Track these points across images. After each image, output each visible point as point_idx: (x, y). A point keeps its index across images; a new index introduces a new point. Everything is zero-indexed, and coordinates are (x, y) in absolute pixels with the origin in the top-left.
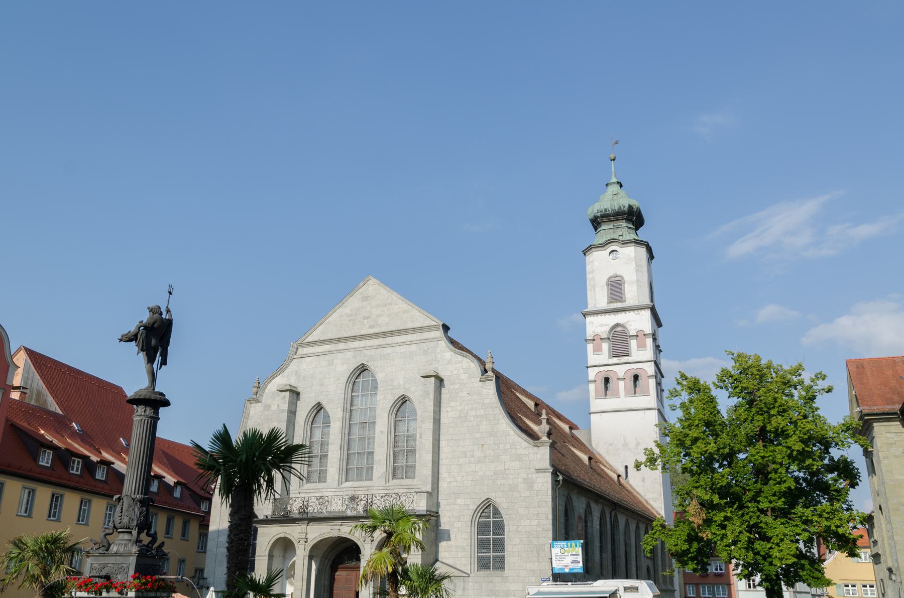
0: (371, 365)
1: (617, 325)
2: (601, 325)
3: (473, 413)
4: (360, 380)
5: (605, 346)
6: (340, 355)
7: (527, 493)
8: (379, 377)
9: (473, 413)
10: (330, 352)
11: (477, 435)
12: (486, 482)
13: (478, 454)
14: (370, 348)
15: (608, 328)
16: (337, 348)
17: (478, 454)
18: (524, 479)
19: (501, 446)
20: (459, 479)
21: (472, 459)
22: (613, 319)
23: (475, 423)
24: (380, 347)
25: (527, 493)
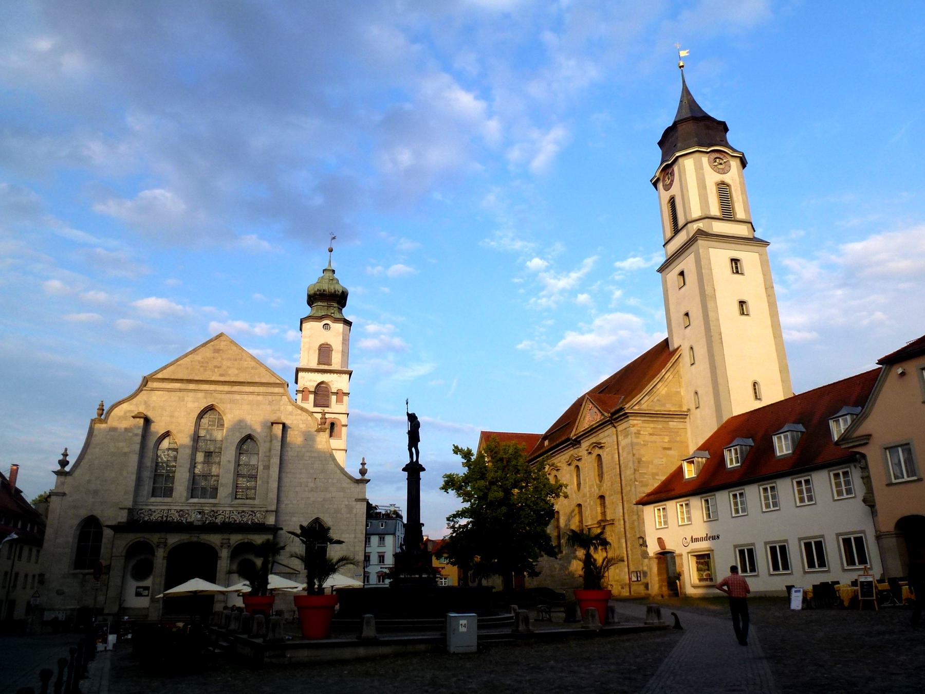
0: (220, 407)
1: (322, 383)
2: (310, 381)
5: (312, 397)
9: (308, 454)
11: (312, 471)
15: (315, 384)
20: (295, 502)
22: (320, 378)
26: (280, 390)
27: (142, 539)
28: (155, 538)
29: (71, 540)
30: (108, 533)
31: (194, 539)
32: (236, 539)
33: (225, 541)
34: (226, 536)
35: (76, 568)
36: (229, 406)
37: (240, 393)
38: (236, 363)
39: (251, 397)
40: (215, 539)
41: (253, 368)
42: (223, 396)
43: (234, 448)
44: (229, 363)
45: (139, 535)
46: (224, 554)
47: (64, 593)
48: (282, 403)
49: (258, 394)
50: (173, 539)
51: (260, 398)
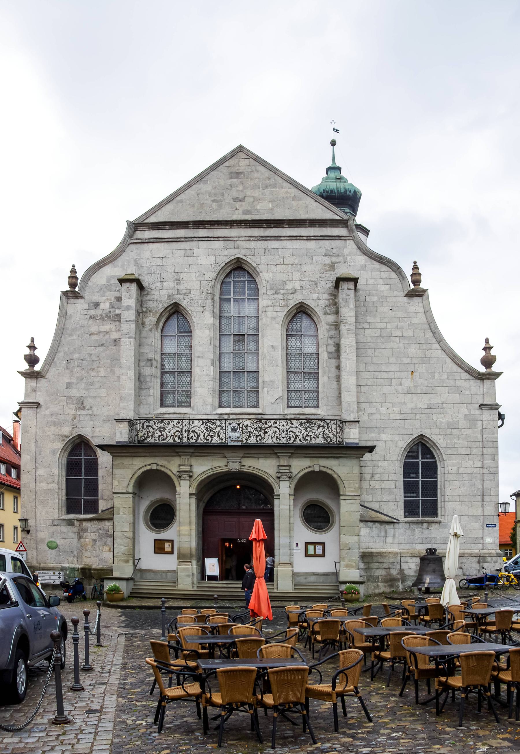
3: (398, 333)
4: (231, 279)
6: (203, 244)
7: (470, 432)
8: (265, 277)
10: (187, 239)
12: (418, 416)
13: (407, 383)
14: (250, 238)
16: (196, 235)
17: (407, 383)
18: (465, 415)
19: (437, 375)
20: (383, 410)
21: (400, 389)
23: (401, 346)
24: (264, 238)
25: (470, 432)
26: (342, 231)
27: (154, 467)
28: (172, 466)
29: (56, 471)
30: (104, 459)
31: (234, 466)
32: (300, 466)
33: (282, 469)
34: (283, 461)
35: (69, 512)
36: (264, 259)
37: (277, 238)
38: (267, 192)
39: (296, 244)
40: (265, 467)
41: (294, 198)
42: (253, 244)
43: (278, 326)
44: (256, 193)
45: (149, 460)
46: (284, 490)
47: (57, 546)
48: (347, 251)
49: (309, 238)
50: (203, 467)
51: (312, 244)
